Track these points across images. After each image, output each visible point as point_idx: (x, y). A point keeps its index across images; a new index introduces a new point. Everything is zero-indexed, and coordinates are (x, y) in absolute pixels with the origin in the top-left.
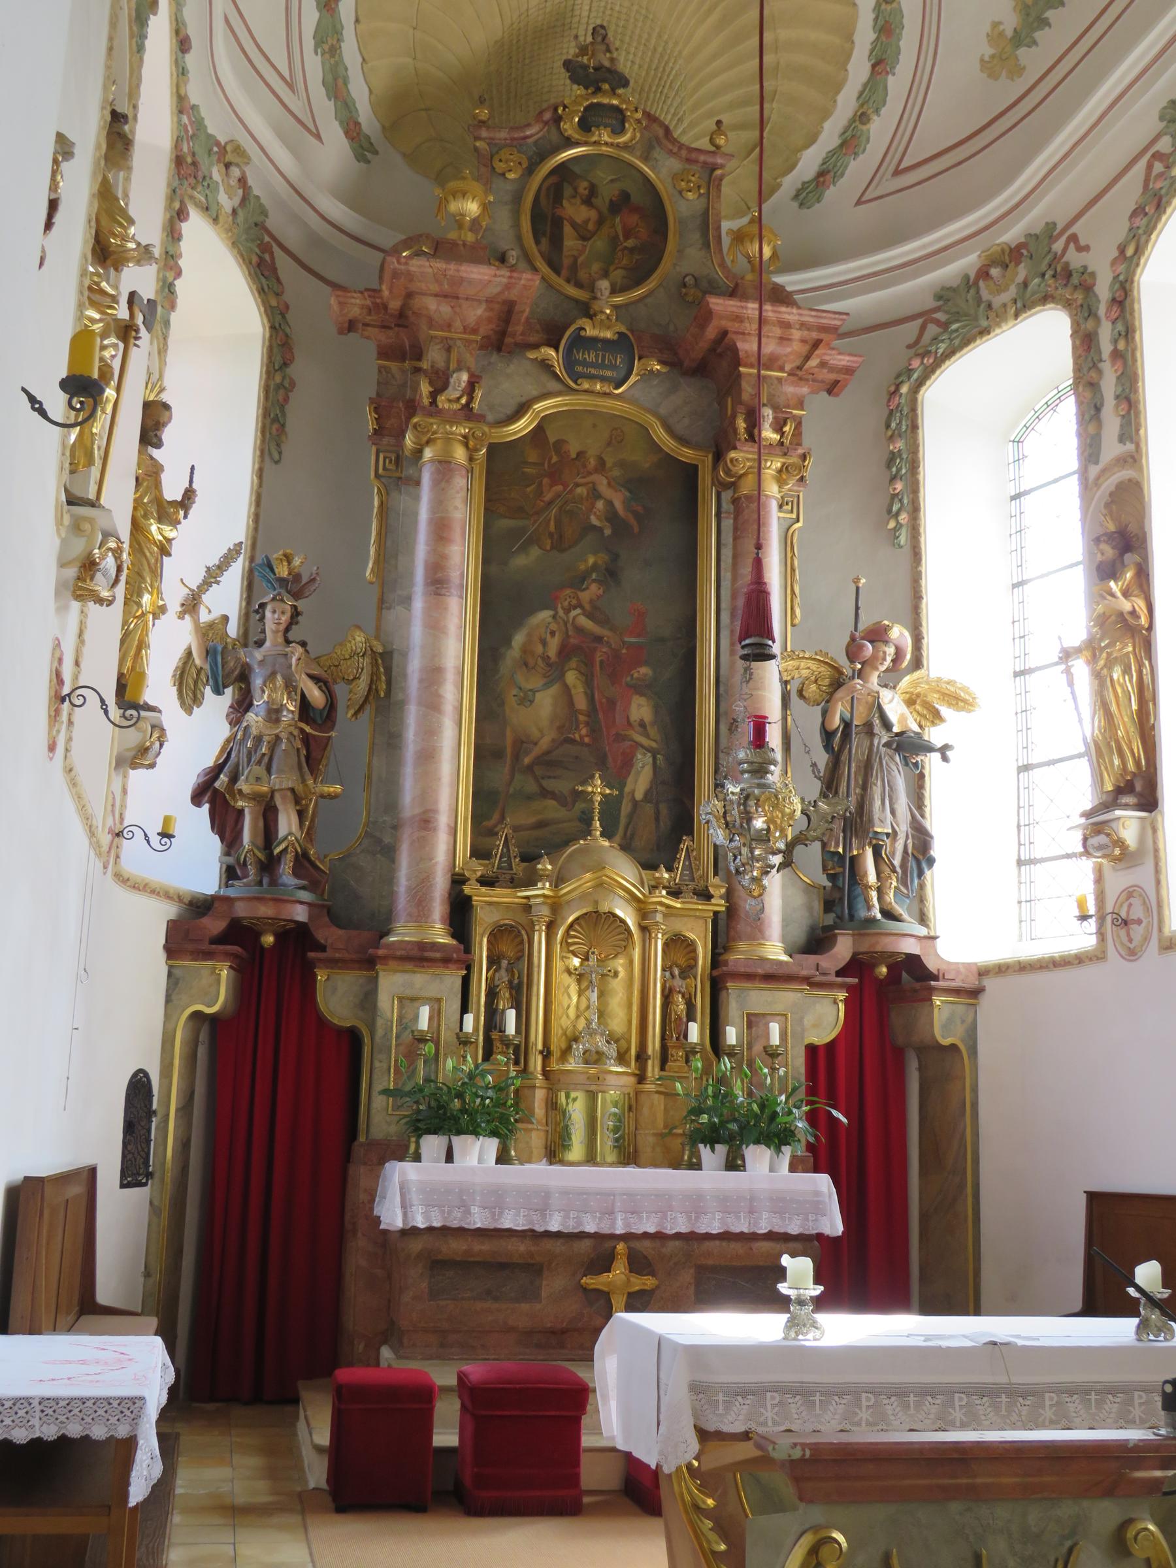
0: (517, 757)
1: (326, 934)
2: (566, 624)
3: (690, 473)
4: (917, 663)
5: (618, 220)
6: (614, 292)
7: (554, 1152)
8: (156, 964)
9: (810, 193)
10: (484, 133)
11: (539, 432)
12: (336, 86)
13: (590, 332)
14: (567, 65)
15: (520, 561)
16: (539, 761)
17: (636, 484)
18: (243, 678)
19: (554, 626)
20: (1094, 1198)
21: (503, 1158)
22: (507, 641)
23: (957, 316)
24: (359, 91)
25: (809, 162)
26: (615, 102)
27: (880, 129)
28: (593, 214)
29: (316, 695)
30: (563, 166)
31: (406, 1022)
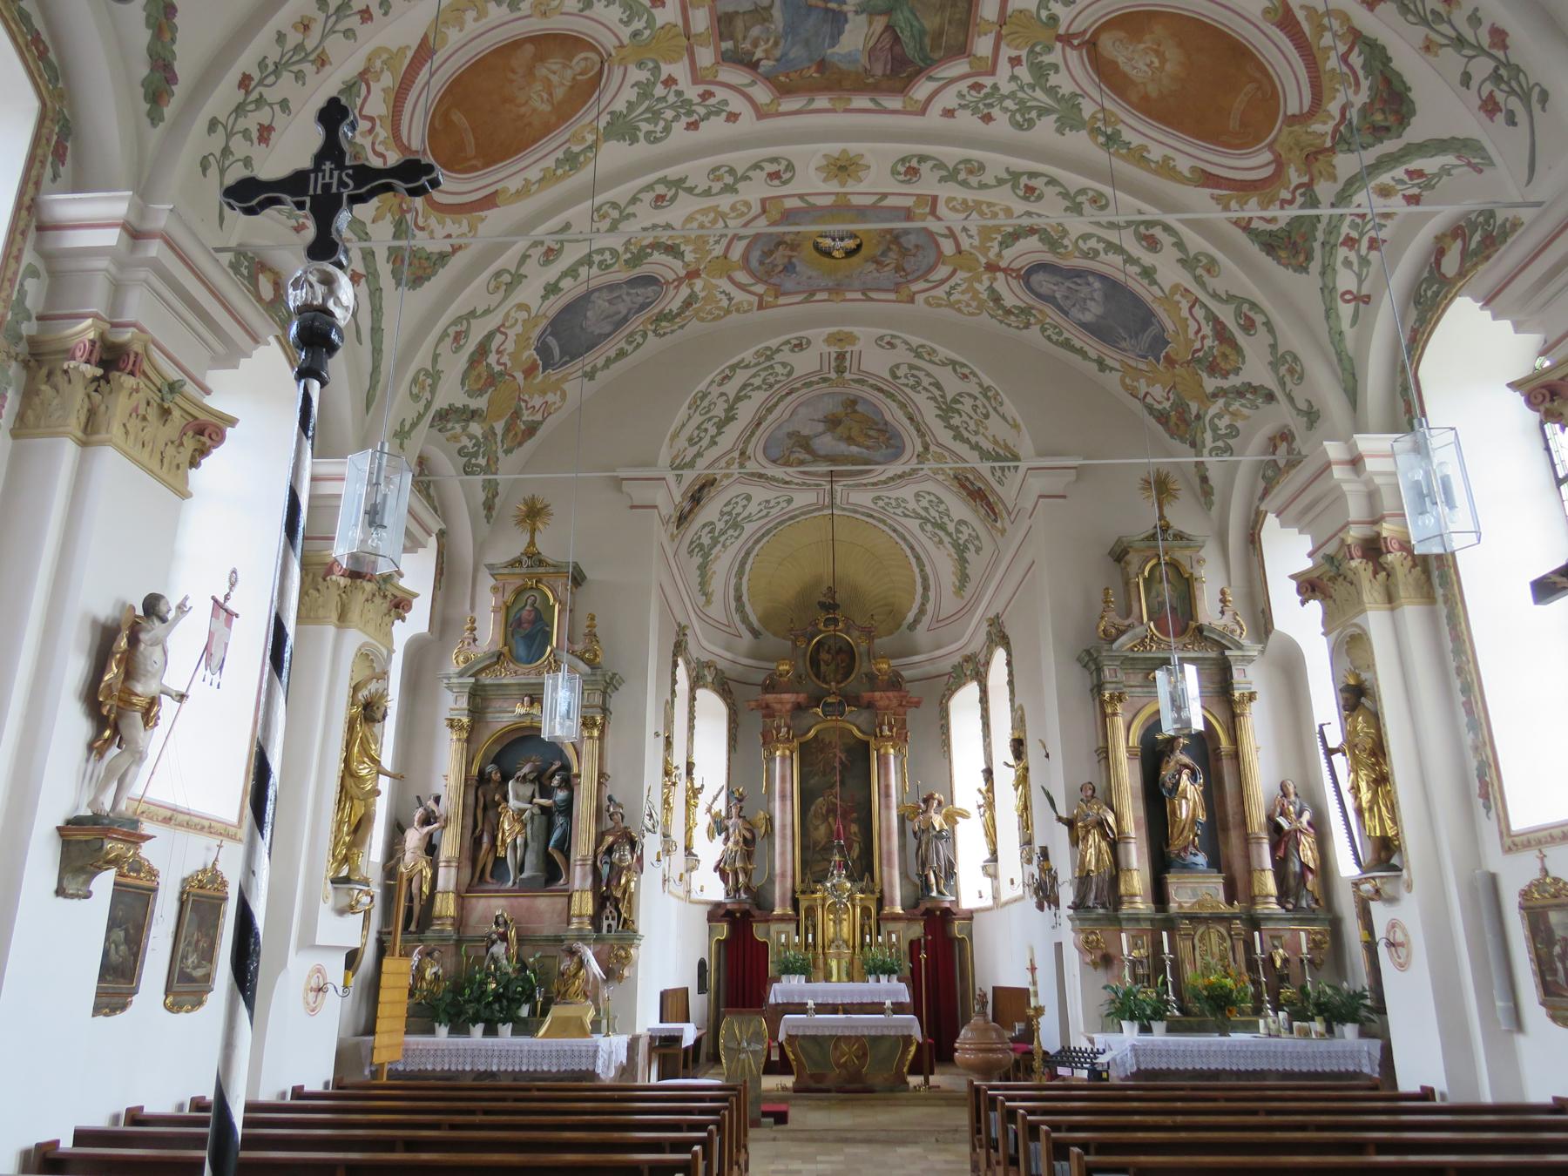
1: (756, 913)
3: (867, 744)
4: (952, 803)
6: (838, 683)
7: (828, 978)
8: (706, 925)
9: (912, 627)
11: (816, 736)
12: (745, 619)
13: (830, 700)
15: (812, 782)
17: (849, 750)
18: (727, 829)
20: (994, 989)
21: (808, 981)
23: (958, 676)
24: (753, 619)
25: (910, 617)
27: (930, 607)
29: (748, 835)
31: (779, 939)
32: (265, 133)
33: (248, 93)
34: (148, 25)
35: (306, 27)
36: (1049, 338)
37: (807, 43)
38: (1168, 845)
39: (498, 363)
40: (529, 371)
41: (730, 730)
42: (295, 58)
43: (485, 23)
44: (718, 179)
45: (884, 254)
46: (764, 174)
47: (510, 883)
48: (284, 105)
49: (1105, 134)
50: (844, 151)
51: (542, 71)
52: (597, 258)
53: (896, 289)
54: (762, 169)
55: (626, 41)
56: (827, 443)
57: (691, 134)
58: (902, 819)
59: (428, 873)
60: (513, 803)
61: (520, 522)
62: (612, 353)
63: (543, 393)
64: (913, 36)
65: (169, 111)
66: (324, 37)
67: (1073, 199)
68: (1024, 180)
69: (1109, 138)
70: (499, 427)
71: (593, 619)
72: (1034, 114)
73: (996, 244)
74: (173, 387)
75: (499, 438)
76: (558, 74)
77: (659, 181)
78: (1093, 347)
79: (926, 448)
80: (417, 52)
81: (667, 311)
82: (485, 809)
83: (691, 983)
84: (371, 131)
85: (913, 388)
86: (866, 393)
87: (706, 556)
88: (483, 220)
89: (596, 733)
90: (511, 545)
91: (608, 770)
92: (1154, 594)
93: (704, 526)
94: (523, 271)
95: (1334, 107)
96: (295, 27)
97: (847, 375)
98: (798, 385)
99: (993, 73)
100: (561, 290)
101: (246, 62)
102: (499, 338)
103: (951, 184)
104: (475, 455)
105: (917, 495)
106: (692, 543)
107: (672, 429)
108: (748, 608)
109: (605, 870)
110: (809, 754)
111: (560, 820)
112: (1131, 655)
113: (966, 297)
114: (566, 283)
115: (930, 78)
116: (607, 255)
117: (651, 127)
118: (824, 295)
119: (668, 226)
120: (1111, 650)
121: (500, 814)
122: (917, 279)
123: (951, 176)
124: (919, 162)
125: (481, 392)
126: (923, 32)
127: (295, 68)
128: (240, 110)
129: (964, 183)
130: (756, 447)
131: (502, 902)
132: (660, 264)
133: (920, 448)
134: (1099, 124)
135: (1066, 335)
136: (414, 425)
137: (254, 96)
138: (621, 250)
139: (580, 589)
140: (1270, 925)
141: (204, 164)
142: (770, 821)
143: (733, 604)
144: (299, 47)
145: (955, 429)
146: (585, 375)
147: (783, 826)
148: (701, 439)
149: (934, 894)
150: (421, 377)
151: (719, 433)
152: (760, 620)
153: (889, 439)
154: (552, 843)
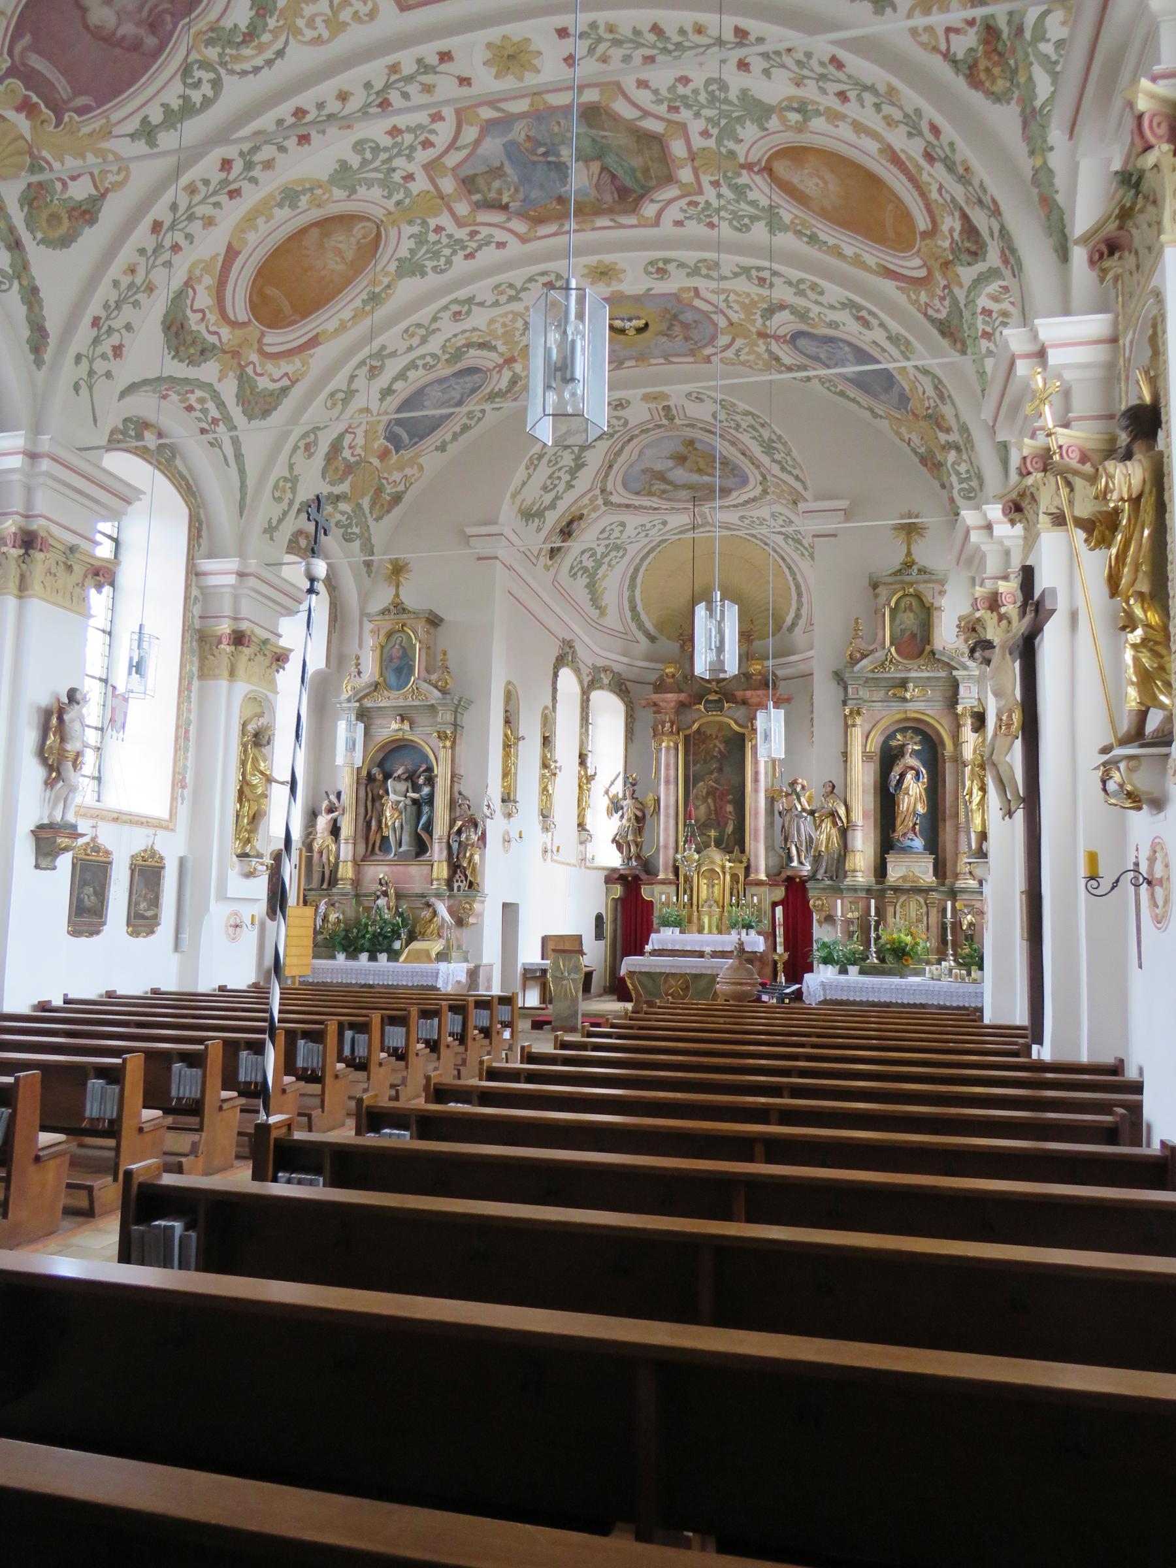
1: (644, 876)
3: (743, 735)
7: (700, 931)
8: (604, 886)
9: (791, 629)
11: (699, 729)
12: (641, 626)
13: (711, 697)
17: (727, 742)
24: (649, 626)
25: (789, 620)
27: (804, 611)
32: (118, 351)
33: (99, 329)
34: (24, 303)
35: (133, 271)
36: (828, 389)
37: (542, 186)
38: (894, 831)
39: (353, 455)
40: (384, 455)
41: (627, 725)
42: (130, 293)
43: (273, 224)
44: (502, 293)
45: (669, 329)
46: (539, 285)
48: (128, 327)
49: (806, 235)
50: (599, 261)
51: (330, 243)
52: (420, 363)
53: (692, 353)
54: (536, 281)
55: (392, 209)
56: (680, 475)
57: (470, 262)
58: (771, 801)
60: (392, 797)
61: (388, 579)
62: (457, 429)
63: (401, 469)
64: (625, 172)
65: (48, 356)
66: (148, 273)
67: (797, 286)
68: (754, 273)
69: (809, 237)
70: (366, 503)
71: (445, 654)
72: (746, 221)
73: (758, 317)
74: (73, 549)
75: (367, 511)
76: (345, 243)
77: (451, 302)
78: (865, 400)
79: (764, 478)
80: (226, 256)
81: (497, 389)
82: (373, 800)
83: (587, 932)
84: (203, 319)
85: (737, 429)
86: (698, 434)
87: (592, 576)
88: (311, 356)
89: (448, 744)
90: (383, 597)
91: (461, 771)
92: (897, 622)
93: (583, 552)
94: (353, 387)
95: (945, 228)
96: (125, 273)
97: (677, 421)
98: (637, 432)
99: (700, 192)
100: (395, 391)
101: (95, 308)
102: (348, 438)
103: (697, 278)
104: (350, 525)
105: (773, 515)
106: (572, 568)
107: (511, 489)
108: (644, 617)
109: (455, 846)
110: (694, 744)
111: (426, 809)
112: (871, 675)
113: (752, 357)
114: (398, 385)
115: (652, 201)
116: (428, 359)
117: (435, 263)
118: (633, 363)
119: (474, 329)
120: (853, 672)
121: (383, 805)
122: (706, 346)
123: (695, 272)
124: (665, 263)
125: (342, 480)
126: (633, 170)
127: (131, 300)
128: (96, 341)
129: (708, 277)
130: (614, 482)
131: (386, 869)
132: (475, 357)
133: (760, 478)
134: (799, 228)
135: (840, 388)
136: (280, 521)
137: (105, 328)
138: (439, 353)
139: (439, 628)
140: (965, 896)
141: (77, 388)
142: (658, 801)
143: (628, 614)
144: (131, 285)
145: (779, 462)
146: (437, 449)
147: (667, 807)
148: (556, 486)
149: (795, 864)
150: (281, 484)
151: (574, 478)
152: (656, 627)
153: (733, 470)
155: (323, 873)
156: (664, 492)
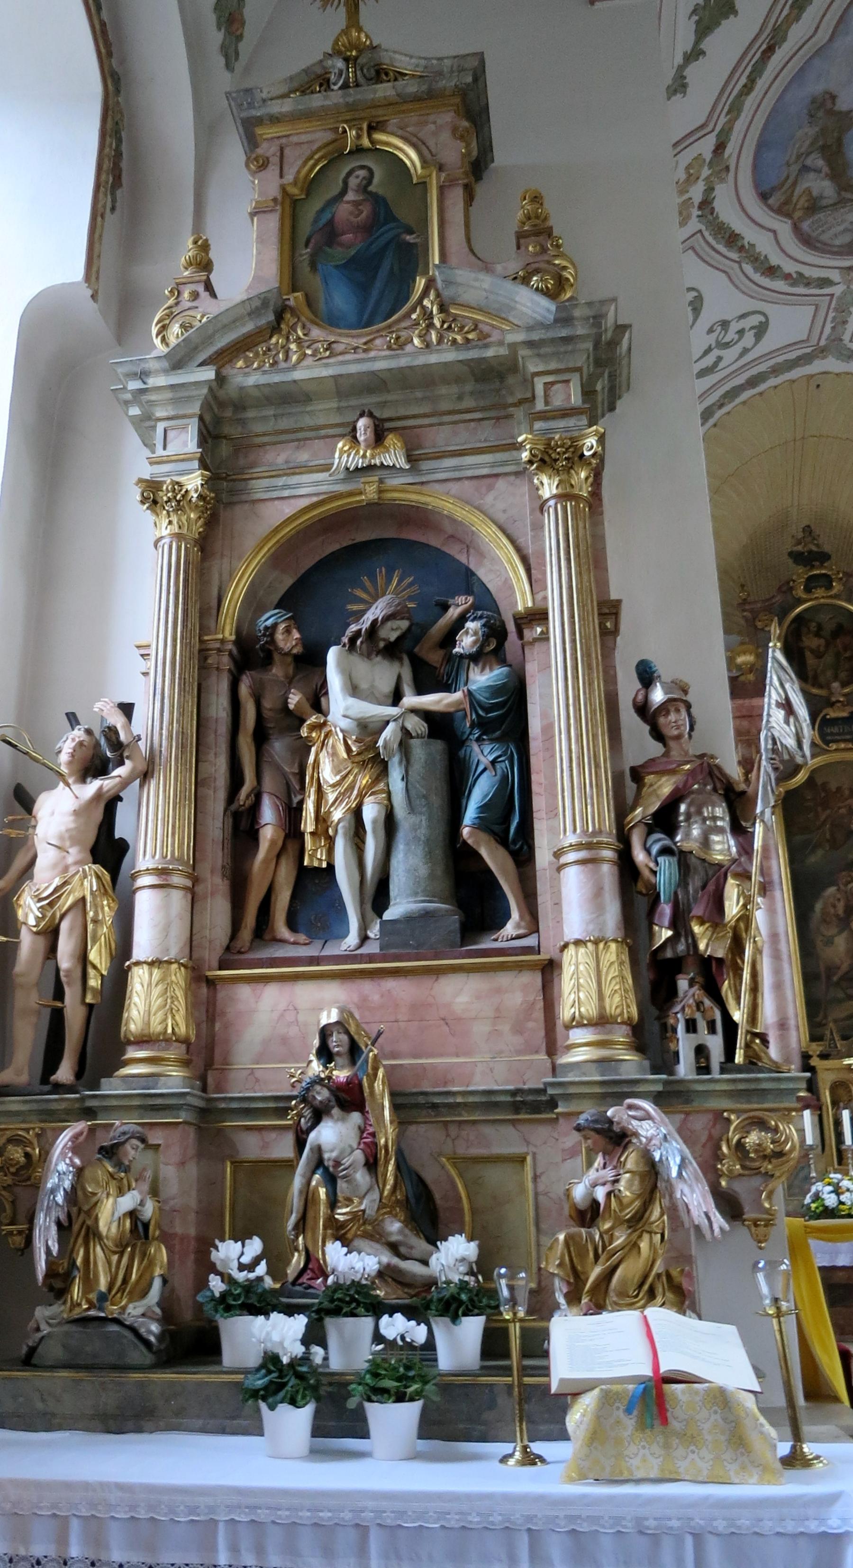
0: (829, 978)
2: (846, 892)
5: (838, 641)
10: (747, 607)
14: (791, 554)
16: (843, 978)
19: (839, 896)
22: (811, 908)
26: (823, 572)
28: (822, 642)
30: (799, 617)
47: (352, 939)
59: (107, 912)
82: (261, 737)
154: (470, 814)
155: (57, 1018)
156: (814, 207)
